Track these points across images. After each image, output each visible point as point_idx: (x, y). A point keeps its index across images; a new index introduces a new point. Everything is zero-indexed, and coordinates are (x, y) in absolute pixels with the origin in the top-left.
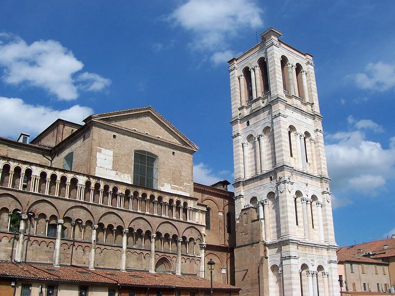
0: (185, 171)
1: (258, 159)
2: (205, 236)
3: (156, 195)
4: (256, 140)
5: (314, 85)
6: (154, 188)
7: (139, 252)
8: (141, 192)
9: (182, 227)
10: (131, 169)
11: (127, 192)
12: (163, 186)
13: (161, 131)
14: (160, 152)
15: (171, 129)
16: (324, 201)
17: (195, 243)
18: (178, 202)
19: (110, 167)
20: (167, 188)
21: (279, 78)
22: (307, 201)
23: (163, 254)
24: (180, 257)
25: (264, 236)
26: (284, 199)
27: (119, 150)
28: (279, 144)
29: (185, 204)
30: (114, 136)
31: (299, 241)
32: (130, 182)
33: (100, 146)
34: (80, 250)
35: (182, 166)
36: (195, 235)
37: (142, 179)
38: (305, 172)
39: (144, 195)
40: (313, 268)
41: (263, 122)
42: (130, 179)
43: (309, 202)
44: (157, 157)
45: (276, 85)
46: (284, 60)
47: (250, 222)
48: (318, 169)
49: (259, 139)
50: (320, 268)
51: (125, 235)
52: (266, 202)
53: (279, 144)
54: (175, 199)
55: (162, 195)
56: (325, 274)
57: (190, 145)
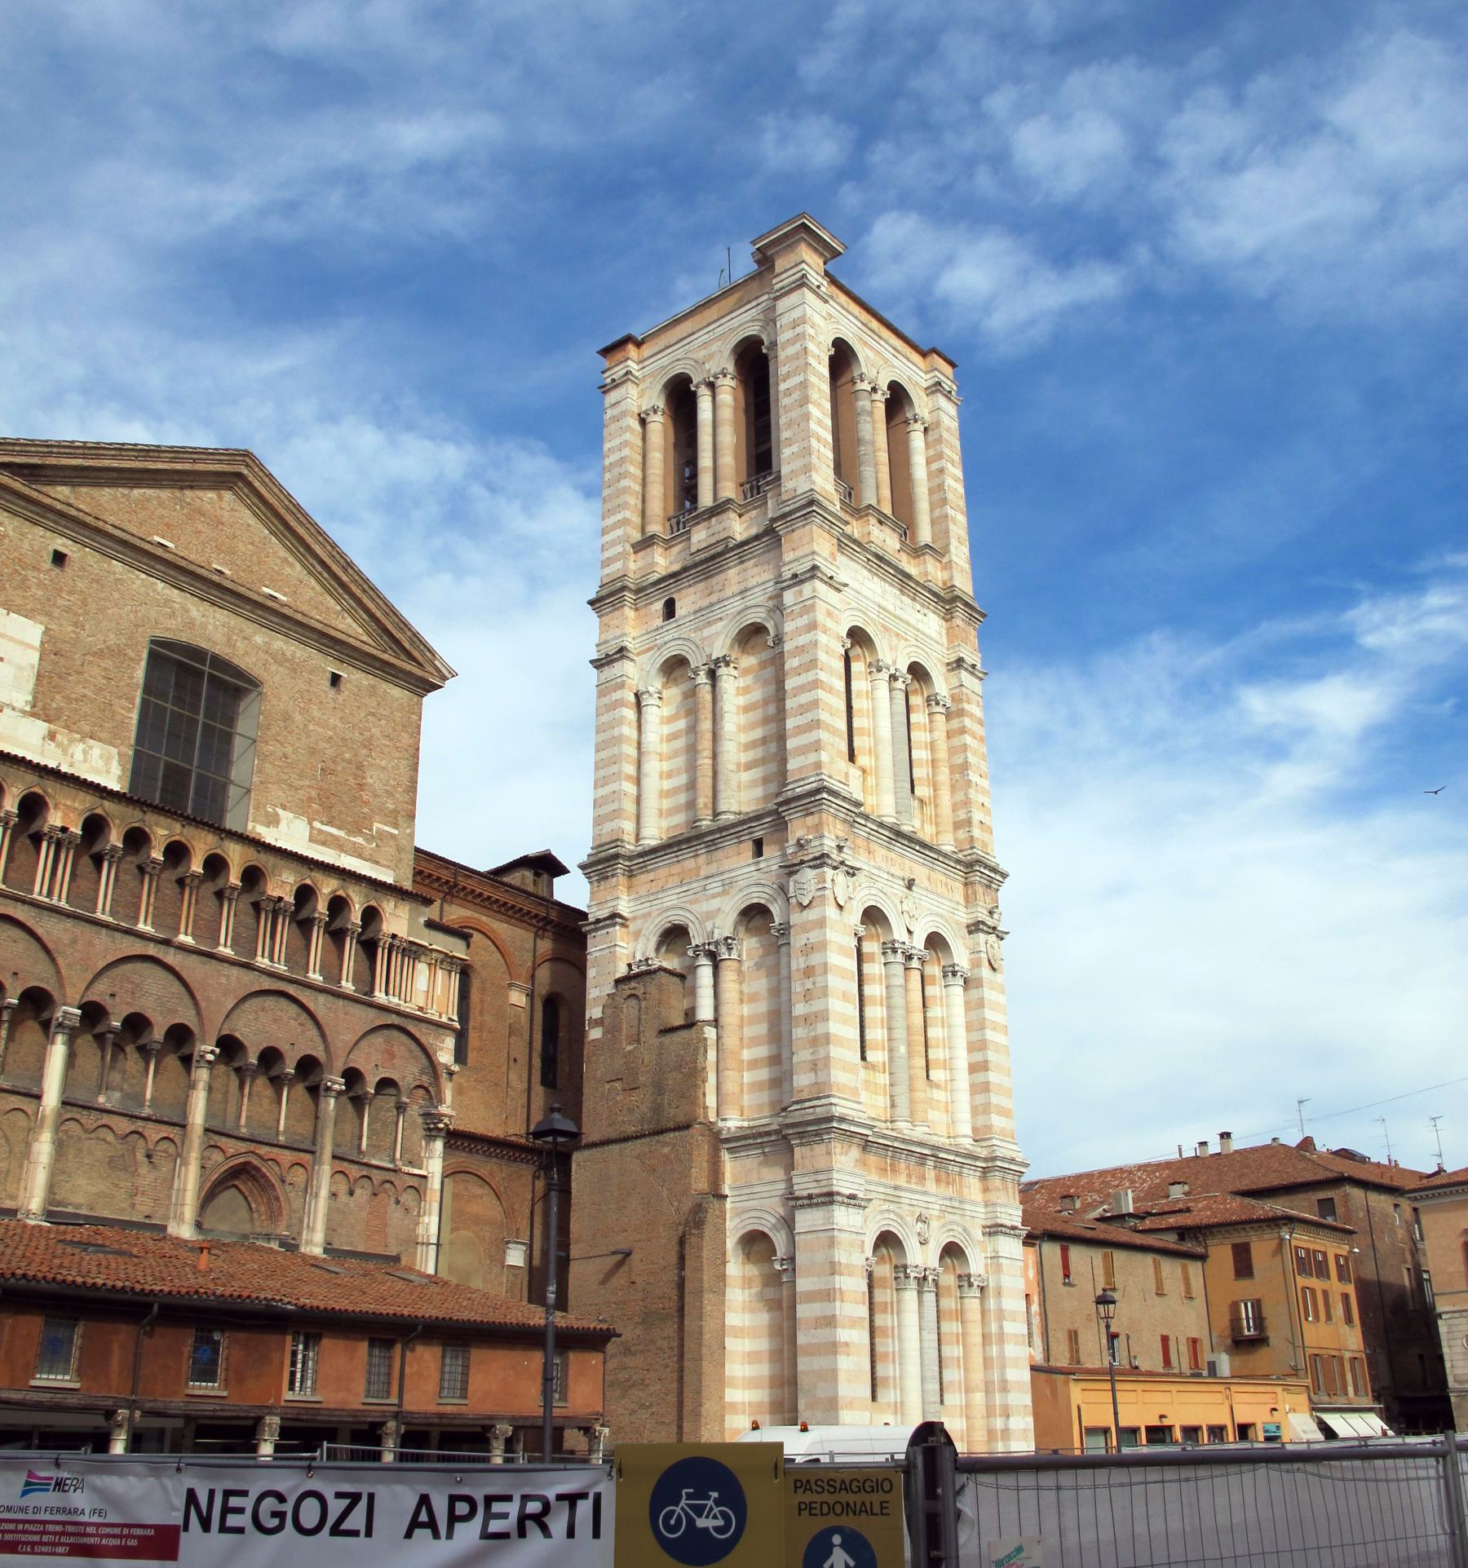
0: (385, 768)
1: (705, 762)
2: (451, 1074)
3: (237, 857)
4: (702, 678)
5: (956, 479)
6: (230, 823)
7: (123, 1125)
8: (162, 832)
9: (346, 1023)
10: (122, 725)
11: (94, 826)
12: (273, 821)
13: (288, 570)
14: (273, 668)
15: (334, 567)
16: (976, 964)
17: (401, 1108)
18: (338, 905)
21: (820, 422)
22: (909, 958)
23: (243, 1147)
24: (326, 1170)
25: (711, 1101)
26: (814, 936)
27: (76, 624)
28: (805, 698)
30: (59, 558)
31: (871, 1127)
32: (113, 779)
35: (368, 744)
36: (407, 1072)
37: (176, 778)
39: (177, 852)
40: (922, 1256)
41: (736, 605)
42: (116, 769)
45: (807, 451)
46: (842, 358)
47: (650, 1036)
48: (957, 826)
49: (712, 675)
50: (952, 1251)
51: (60, 1038)
52: (730, 949)
53: (805, 698)
54: (327, 887)
56: (970, 1285)
57: (416, 654)
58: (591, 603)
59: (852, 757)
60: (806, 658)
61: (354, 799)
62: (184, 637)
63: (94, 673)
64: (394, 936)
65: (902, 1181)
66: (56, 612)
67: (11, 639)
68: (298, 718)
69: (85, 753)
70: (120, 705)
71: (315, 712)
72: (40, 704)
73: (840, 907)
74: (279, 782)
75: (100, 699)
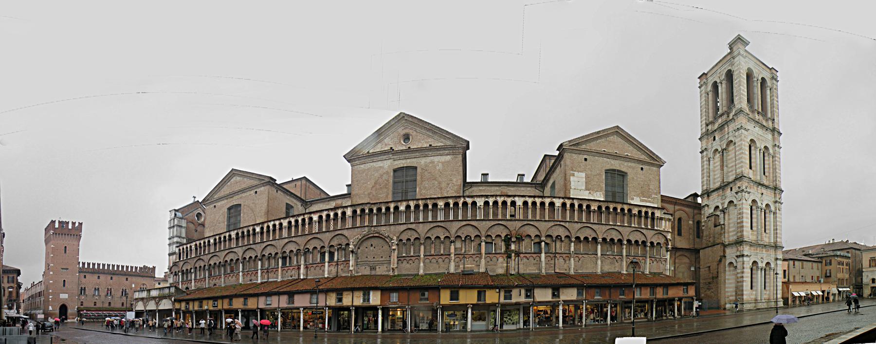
2: (670, 240)
3: (626, 208)
8: (611, 206)
9: (649, 234)
10: (602, 188)
11: (600, 208)
12: (633, 199)
13: (630, 148)
15: (639, 146)
17: (661, 247)
18: (646, 213)
20: (636, 201)
24: (648, 259)
29: (653, 214)
30: (586, 159)
34: (561, 260)
35: (650, 180)
36: (662, 241)
37: (614, 194)
38: (762, 183)
39: (615, 209)
40: (762, 265)
42: (602, 196)
43: (763, 210)
44: (626, 173)
54: (644, 210)
55: (631, 207)
57: (657, 160)
59: (751, 168)
60: (740, 147)
62: (611, 168)
65: (758, 252)
68: (635, 178)
71: (638, 176)
74: (633, 191)
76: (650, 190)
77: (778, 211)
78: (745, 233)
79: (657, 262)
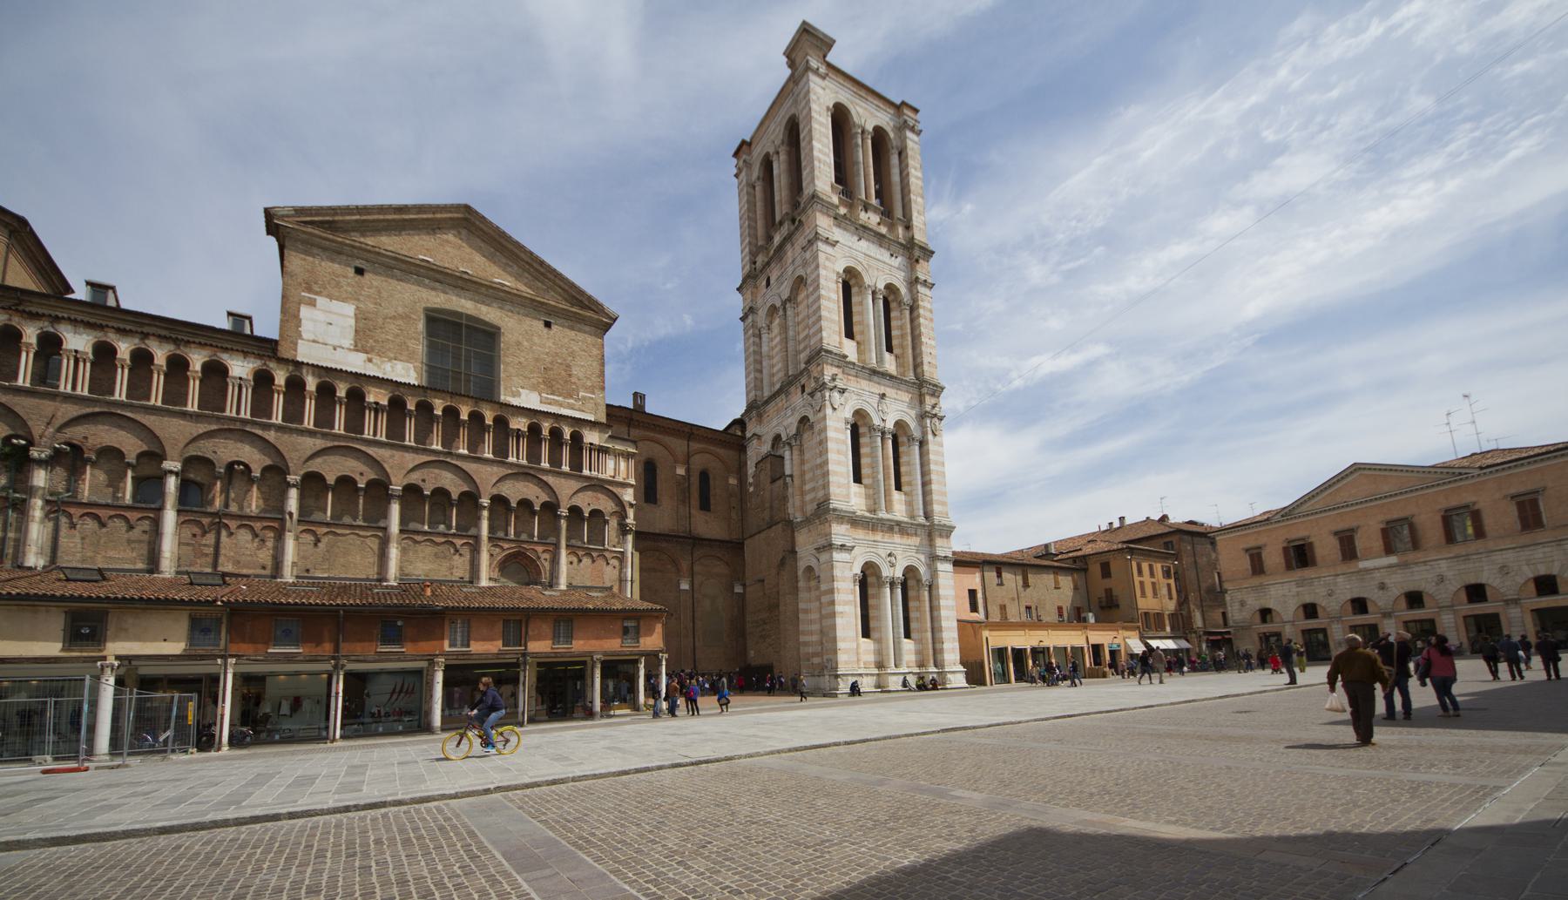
0: (582, 366)
12: (518, 395)
19: (348, 342)
26: (822, 425)
27: (376, 304)
33: (309, 290)
35: (572, 354)
36: (606, 505)
58: (738, 289)
61: (566, 382)
63: (392, 327)
64: (591, 444)
66: (362, 298)
67: (335, 313)
68: (526, 343)
69: (392, 367)
70: (412, 344)
71: (536, 340)
72: (359, 345)
73: (834, 409)
74: (517, 376)
75: (398, 340)
76: (574, 380)
77: (930, 437)
78: (833, 489)
79: (594, 561)
